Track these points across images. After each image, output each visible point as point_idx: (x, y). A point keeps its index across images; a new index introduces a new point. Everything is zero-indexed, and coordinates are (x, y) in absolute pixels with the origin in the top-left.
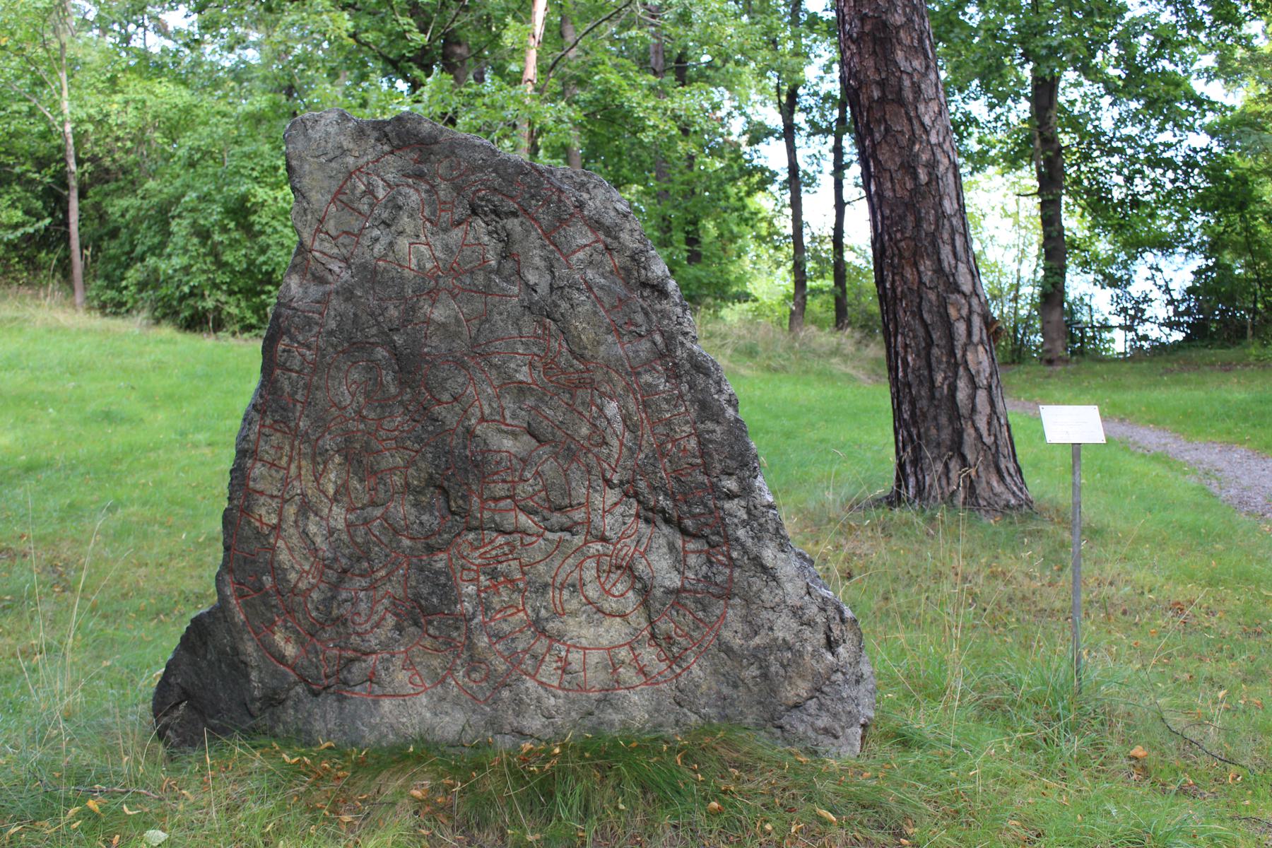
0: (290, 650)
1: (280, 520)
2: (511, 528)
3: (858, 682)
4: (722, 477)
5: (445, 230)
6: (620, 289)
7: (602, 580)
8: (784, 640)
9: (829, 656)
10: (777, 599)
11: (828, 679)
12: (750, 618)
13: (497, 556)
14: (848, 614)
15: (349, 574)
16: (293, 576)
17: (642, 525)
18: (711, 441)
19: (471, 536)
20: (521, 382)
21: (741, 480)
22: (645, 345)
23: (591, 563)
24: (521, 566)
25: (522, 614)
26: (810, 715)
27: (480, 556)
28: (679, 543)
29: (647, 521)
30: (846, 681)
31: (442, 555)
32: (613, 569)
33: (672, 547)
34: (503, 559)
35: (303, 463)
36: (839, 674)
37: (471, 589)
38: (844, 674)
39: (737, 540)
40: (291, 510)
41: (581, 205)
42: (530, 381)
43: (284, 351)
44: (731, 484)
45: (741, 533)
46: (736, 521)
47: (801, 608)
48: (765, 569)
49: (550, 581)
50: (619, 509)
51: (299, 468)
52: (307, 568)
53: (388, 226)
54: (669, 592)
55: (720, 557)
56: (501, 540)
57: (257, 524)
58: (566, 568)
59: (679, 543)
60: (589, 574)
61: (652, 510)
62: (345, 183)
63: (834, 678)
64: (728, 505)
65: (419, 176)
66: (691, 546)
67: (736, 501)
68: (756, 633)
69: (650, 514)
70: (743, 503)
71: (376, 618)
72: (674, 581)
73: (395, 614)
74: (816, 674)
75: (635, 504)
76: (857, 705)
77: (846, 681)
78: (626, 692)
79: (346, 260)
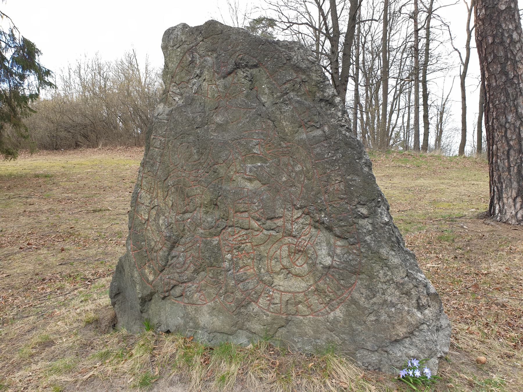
0: (151, 278)
1: (149, 217)
2: (247, 227)
3: (437, 330)
4: (358, 206)
5: (224, 77)
6: (308, 103)
7: (292, 257)
8: (391, 301)
9: (419, 315)
10: (388, 278)
11: (418, 328)
12: (371, 287)
13: (241, 240)
14: (433, 290)
15: (177, 244)
16: (153, 243)
17: (313, 230)
18: (353, 186)
19: (230, 229)
20: (255, 153)
21: (369, 209)
22: (319, 132)
23: (285, 248)
24: (252, 246)
25: (252, 270)
26: (405, 347)
27: (233, 240)
28: (332, 241)
29: (315, 227)
30: (429, 330)
31: (217, 238)
32: (297, 252)
33: (328, 244)
34: (244, 242)
35: (159, 191)
36: (425, 326)
37: (229, 256)
38: (428, 326)
39: (365, 241)
40: (154, 212)
41: (290, 59)
42: (259, 153)
43: (154, 139)
44: (364, 211)
45: (368, 238)
46: (365, 231)
47: (402, 284)
48: (381, 259)
49: (266, 255)
50: (301, 220)
51: (157, 193)
52: (158, 240)
53: (200, 77)
54: (324, 267)
55: (355, 251)
56: (243, 232)
57: (140, 218)
58: (273, 249)
59: (332, 241)
60: (285, 254)
61: (317, 221)
62: (183, 58)
63: (421, 327)
64: (361, 222)
65: (213, 51)
66: (338, 243)
67: (366, 220)
68: (374, 296)
69: (318, 224)
70: (370, 221)
71: (187, 266)
72: (328, 261)
73: (195, 265)
74: (410, 324)
75: (309, 219)
76: (436, 345)
77: (429, 330)
78: (301, 318)
79: (181, 95)
